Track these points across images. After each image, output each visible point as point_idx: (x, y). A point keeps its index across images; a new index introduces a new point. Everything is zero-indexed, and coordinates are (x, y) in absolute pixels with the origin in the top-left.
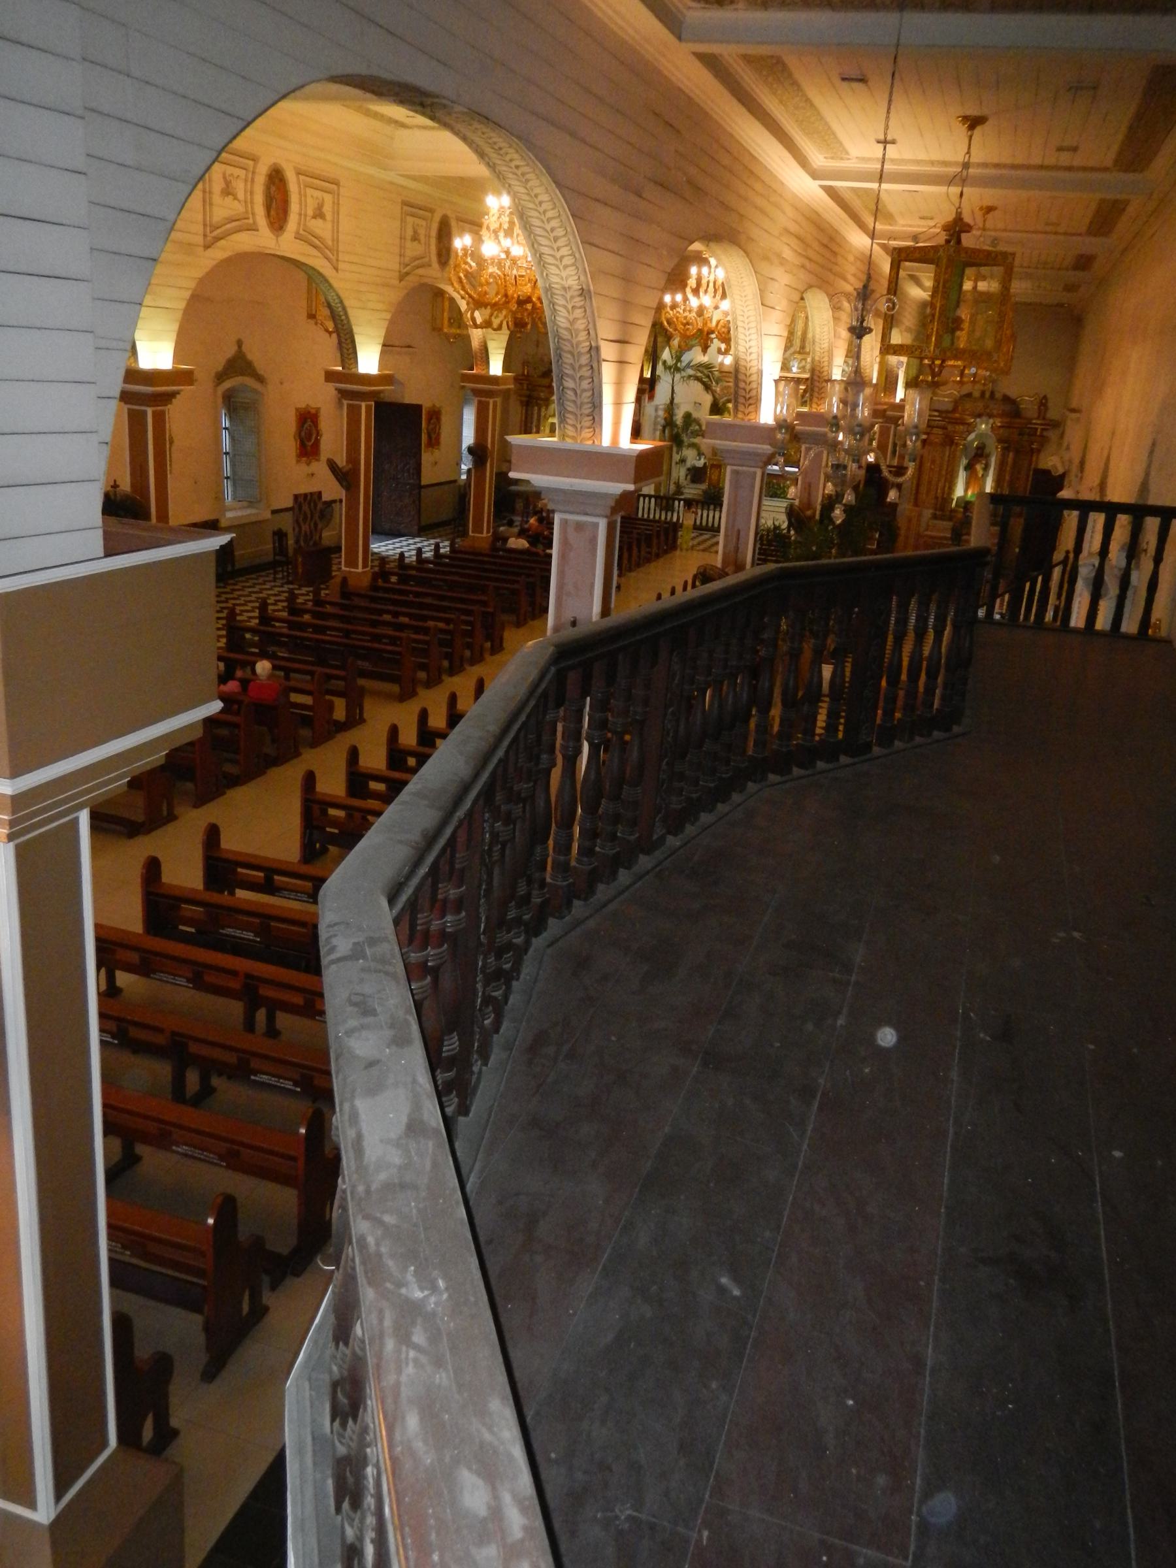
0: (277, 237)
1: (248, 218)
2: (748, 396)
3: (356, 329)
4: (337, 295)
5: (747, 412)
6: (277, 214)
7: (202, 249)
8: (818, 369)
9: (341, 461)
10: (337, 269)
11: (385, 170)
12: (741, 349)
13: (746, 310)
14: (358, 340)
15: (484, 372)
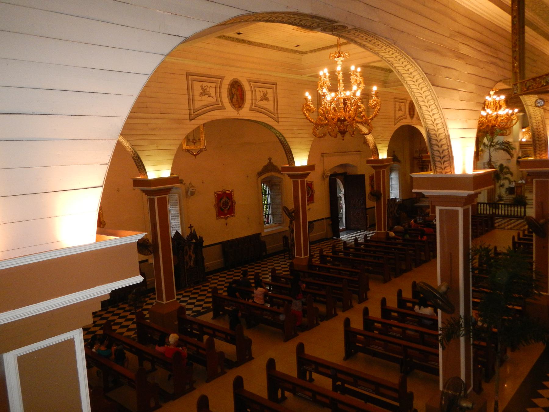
0: (238, 111)
1: (219, 104)
2: (442, 156)
3: (291, 147)
4: (280, 133)
5: (443, 167)
6: (237, 101)
7: (189, 120)
8: (537, 133)
9: (291, 206)
10: (278, 122)
11: (301, 75)
12: (428, 121)
13: (422, 92)
14: (293, 151)
15: (377, 158)
